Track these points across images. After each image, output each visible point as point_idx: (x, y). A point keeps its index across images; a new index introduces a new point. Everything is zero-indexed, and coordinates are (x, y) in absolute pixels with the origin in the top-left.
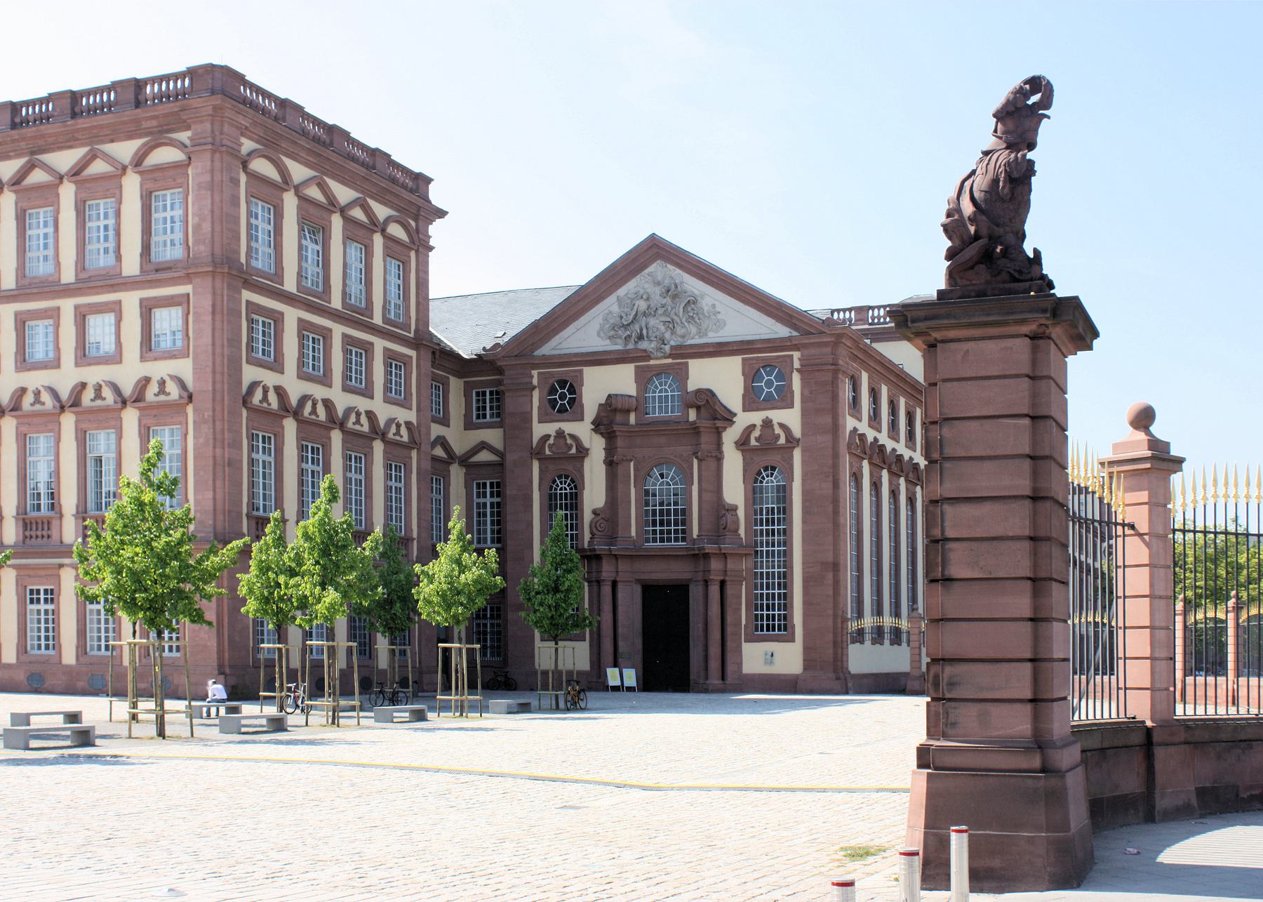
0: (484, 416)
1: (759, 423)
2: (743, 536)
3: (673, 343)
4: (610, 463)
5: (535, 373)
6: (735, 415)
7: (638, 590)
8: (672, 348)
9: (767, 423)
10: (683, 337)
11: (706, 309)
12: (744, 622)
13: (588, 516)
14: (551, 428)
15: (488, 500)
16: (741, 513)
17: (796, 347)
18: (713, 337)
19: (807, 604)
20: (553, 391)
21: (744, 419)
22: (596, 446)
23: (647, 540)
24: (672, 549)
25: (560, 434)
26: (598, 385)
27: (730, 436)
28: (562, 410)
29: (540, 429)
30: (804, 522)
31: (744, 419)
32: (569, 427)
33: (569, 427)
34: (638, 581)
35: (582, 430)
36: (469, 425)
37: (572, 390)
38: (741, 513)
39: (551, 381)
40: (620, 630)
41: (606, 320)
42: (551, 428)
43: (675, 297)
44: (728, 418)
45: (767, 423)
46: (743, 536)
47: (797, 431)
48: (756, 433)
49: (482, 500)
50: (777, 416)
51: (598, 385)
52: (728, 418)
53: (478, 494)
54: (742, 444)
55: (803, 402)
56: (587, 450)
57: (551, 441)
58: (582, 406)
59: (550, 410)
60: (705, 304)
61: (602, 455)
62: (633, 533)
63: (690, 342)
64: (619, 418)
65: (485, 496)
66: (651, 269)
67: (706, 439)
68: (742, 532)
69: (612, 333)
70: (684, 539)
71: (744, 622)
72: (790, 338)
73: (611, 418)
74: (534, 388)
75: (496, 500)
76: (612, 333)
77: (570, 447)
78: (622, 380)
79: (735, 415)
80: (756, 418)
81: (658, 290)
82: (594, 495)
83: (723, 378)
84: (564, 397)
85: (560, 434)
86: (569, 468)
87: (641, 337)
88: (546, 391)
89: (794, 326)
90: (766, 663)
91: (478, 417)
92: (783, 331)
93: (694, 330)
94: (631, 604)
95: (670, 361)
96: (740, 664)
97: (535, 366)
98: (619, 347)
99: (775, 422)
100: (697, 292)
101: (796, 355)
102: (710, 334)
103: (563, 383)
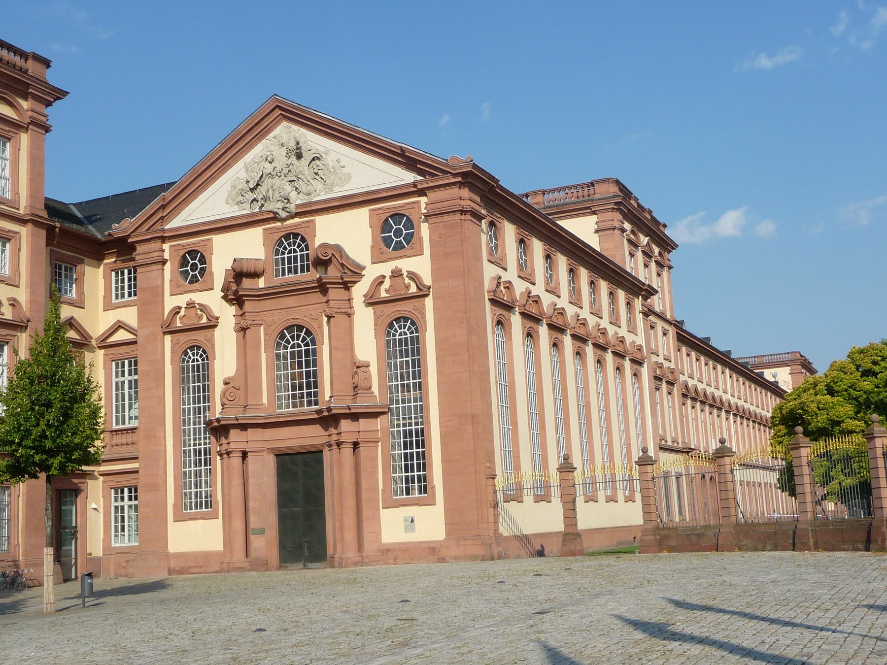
0: (123, 296)
1: (388, 274)
2: (377, 393)
3: (299, 202)
4: (242, 330)
5: (166, 246)
6: (363, 268)
7: (271, 460)
8: (297, 206)
9: (396, 274)
10: (309, 194)
11: (331, 164)
12: (381, 487)
13: (218, 387)
14: (181, 300)
15: (127, 378)
16: (374, 370)
17: (422, 192)
18: (339, 191)
19: (445, 460)
20: (184, 262)
21: (371, 272)
22: (227, 314)
23: (280, 407)
24: (303, 414)
25: (191, 305)
26: (225, 252)
27: (359, 290)
28: (194, 280)
29: (170, 302)
30: (439, 373)
31: (371, 272)
32: (199, 298)
33: (199, 298)
34: (270, 450)
35: (212, 299)
36: (108, 306)
37: (203, 260)
38: (374, 370)
39: (182, 253)
40: (251, 504)
41: (234, 187)
42: (181, 300)
43: (299, 156)
44: (357, 272)
45: (396, 274)
46: (377, 393)
47: (427, 280)
48: (387, 284)
49: (120, 379)
50: (406, 265)
51: (225, 252)
52: (357, 272)
53: (117, 373)
54: (372, 301)
55: (432, 247)
56: (217, 318)
57: (182, 312)
58: (212, 274)
59: (182, 281)
60: (330, 160)
61: (233, 321)
62: (265, 400)
63: (315, 199)
64: (246, 283)
65: (123, 375)
66: (277, 131)
67: (334, 293)
68: (375, 389)
69: (240, 198)
70: (316, 403)
71: (381, 487)
72: (415, 185)
73: (240, 284)
74: (164, 262)
75: (134, 377)
76: (240, 198)
77: (200, 317)
78: (251, 245)
79: (363, 268)
80: (386, 269)
81: (284, 151)
82: (225, 362)
83: (349, 234)
84: (194, 267)
85: (191, 305)
86: (199, 337)
87: (265, 199)
88: (177, 263)
89: (421, 172)
90: (406, 531)
91: (117, 298)
92: (408, 177)
93: (318, 185)
94: (264, 474)
95: (297, 220)
96: (378, 533)
97: (164, 239)
98: (247, 212)
99: (405, 274)
100: (321, 149)
101: (423, 200)
102: (336, 189)
103: (193, 253)
